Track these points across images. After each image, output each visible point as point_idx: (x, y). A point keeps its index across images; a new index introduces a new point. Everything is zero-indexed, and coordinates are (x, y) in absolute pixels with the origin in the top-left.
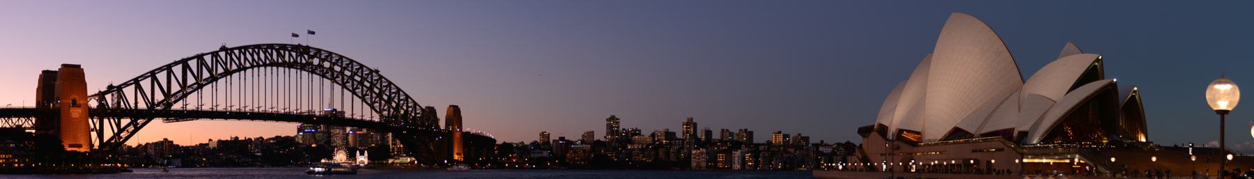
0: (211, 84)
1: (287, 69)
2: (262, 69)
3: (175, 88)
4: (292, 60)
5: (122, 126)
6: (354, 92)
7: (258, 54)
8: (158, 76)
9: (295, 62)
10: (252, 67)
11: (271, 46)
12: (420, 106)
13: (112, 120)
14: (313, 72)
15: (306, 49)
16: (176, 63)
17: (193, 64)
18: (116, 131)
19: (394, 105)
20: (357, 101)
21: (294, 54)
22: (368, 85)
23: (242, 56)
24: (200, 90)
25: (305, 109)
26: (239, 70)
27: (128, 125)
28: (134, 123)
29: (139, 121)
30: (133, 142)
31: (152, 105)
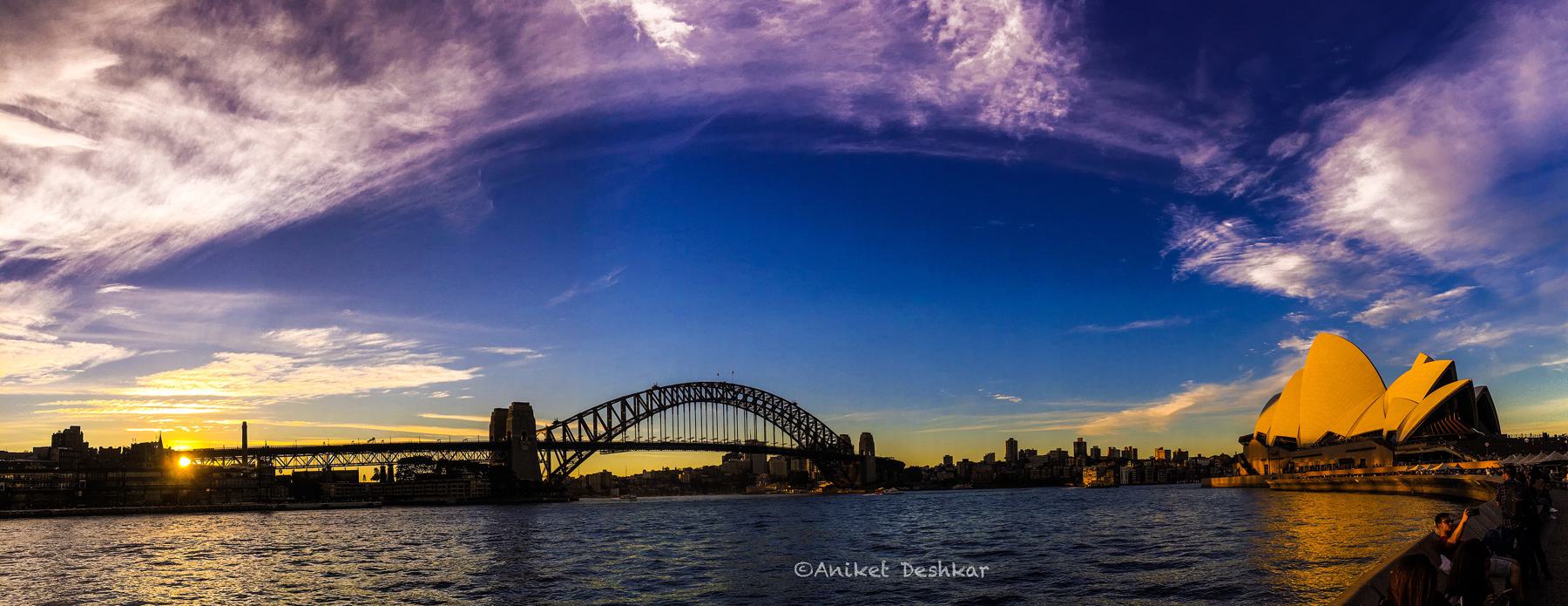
3: (615, 422)
4: (719, 396)
5: (568, 458)
6: (775, 423)
9: (722, 396)
10: (684, 403)
11: (700, 384)
14: (738, 406)
16: (616, 401)
17: (630, 401)
19: (812, 433)
20: (778, 430)
21: (721, 391)
23: (675, 394)
25: (731, 439)
30: (575, 474)
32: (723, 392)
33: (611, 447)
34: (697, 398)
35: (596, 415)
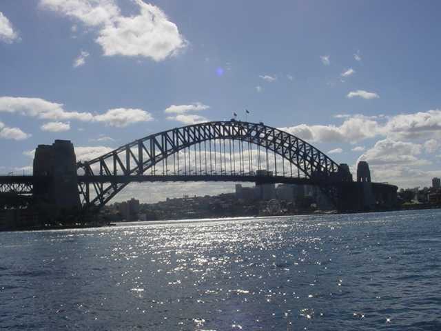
2: (213, 140)
3: (146, 157)
4: (235, 133)
5: (104, 189)
6: (284, 156)
7: (209, 130)
9: (238, 133)
10: (205, 139)
11: (219, 123)
13: (96, 185)
14: (251, 142)
16: (146, 138)
17: (159, 139)
18: (99, 193)
19: (315, 164)
20: (287, 161)
21: (237, 129)
22: (294, 149)
24: (165, 160)
26: (194, 142)
27: (109, 188)
28: (114, 185)
30: (112, 202)
31: (127, 171)
32: (239, 130)
33: (140, 178)
34: (217, 136)
35: (129, 151)
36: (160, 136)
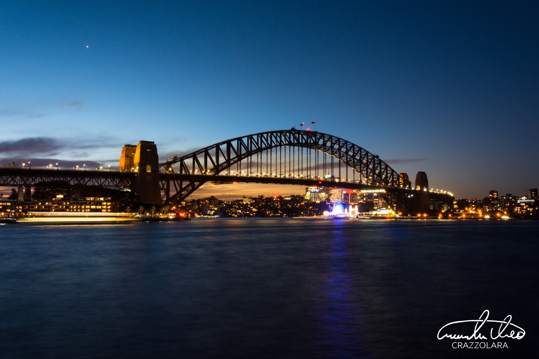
0: (247, 158)
1: (300, 148)
3: (222, 160)
4: (304, 141)
5: (183, 186)
8: (210, 152)
9: (306, 141)
10: (276, 146)
12: (396, 173)
13: (176, 182)
15: (315, 134)
17: (234, 144)
21: (305, 137)
26: (267, 148)
27: (188, 186)
28: (192, 184)
29: (195, 183)
32: (308, 139)
36: (236, 141)
